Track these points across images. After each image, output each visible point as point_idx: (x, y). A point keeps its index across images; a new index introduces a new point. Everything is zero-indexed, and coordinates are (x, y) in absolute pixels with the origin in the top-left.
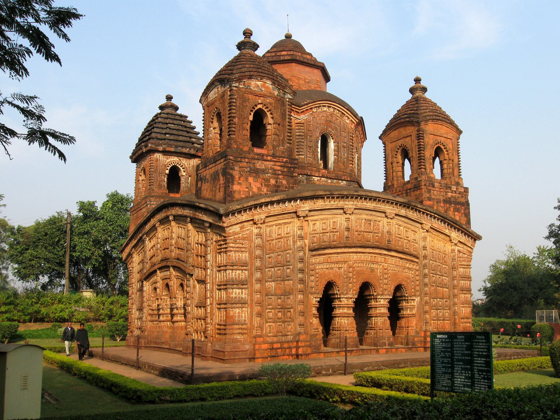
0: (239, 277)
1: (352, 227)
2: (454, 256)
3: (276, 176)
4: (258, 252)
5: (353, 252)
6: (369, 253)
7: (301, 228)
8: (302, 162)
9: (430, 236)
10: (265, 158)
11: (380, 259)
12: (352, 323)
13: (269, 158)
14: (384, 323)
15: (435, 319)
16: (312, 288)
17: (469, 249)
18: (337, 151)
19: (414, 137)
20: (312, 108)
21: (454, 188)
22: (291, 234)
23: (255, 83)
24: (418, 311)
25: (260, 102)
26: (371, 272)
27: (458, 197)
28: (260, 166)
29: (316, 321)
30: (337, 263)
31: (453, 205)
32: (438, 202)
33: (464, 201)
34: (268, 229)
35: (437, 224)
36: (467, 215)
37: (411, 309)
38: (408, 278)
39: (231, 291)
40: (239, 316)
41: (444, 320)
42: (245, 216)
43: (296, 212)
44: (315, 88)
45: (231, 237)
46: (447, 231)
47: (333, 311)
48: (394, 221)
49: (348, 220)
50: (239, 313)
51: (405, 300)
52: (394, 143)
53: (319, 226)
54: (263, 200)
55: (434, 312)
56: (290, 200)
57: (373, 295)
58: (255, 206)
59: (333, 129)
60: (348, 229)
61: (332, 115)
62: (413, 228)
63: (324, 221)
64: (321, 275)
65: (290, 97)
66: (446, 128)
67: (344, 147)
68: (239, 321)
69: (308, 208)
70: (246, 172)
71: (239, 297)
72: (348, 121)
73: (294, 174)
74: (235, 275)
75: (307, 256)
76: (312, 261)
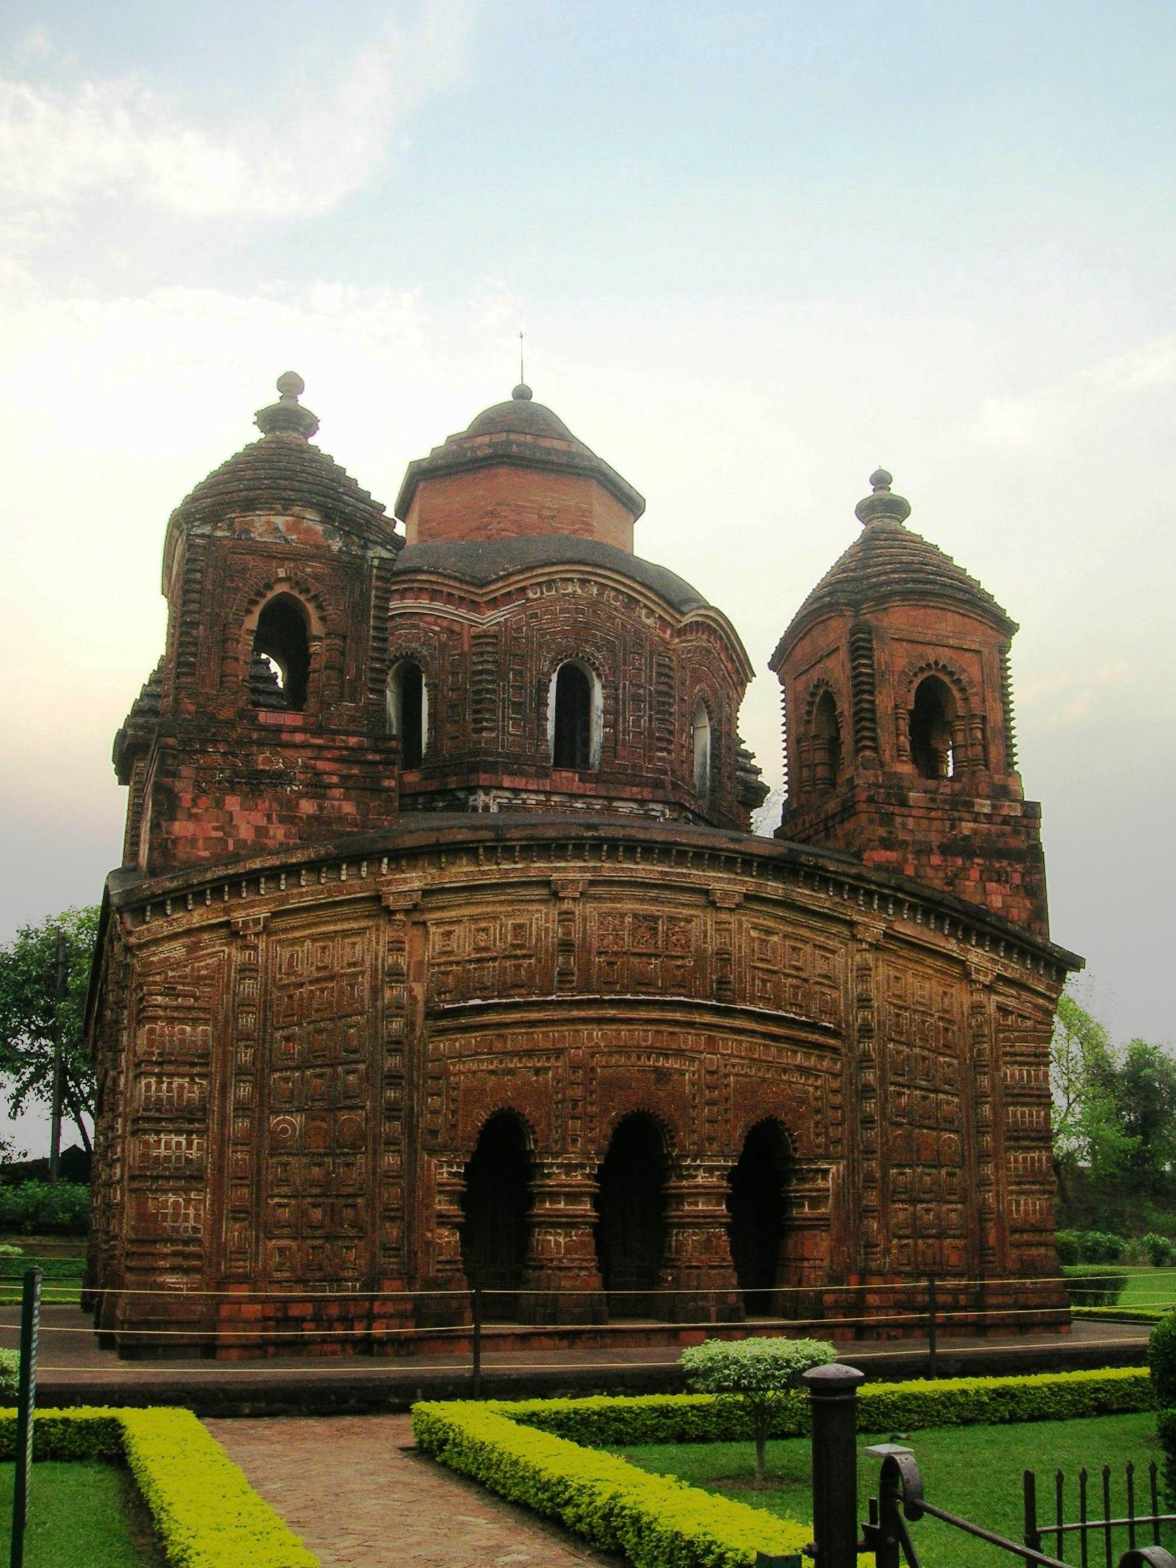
0: (180, 1096)
1: (584, 939)
2: (980, 1026)
3: (322, 791)
4: (248, 1021)
5: (585, 1021)
7: (397, 946)
8: (487, 753)
9: (889, 963)
10: (285, 737)
11: (689, 1040)
12: (583, 1245)
13: (299, 738)
14: (708, 1245)
16: (434, 1133)
17: (1041, 1001)
18: (612, 713)
19: (843, 655)
20: (524, 589)
21: (984, 806)
22: (368, 964)
23: (268, 522)
24: (837, 1206)
25: (282, 573)
26: (658, 1081)
28: (268, 761)
29: (448, 1237)
30: (529, 1053)
31: (977, 860)
32: (923, 850)
33: (1024, 846)
34: (284, 953)
36: (1035, 891)
37: (815, 1202)
38: (802, 1101)
39: (152, 1138)
40: (176, 1214)
42: (198, 917)
43: (377, 898)
44: (575, 531)
45: (158, 978)
46: (951, 946)
47: (531, 1205)
49: (566, 917)
50: (176, 1204)
51: (796, 1171)
52: (804, 678)
53: (463, 941)
54: (257, 864)
55: (901, 1212)
56: (354, 861)
57: (670, 1154)
58: (234, 883)
59: (598, 649)
60: (566, 946)
61: (594, 604)
62: (821, 939)
63: (483, 925)
64: (467, 1092)
65: (386, 555)
66: (957, 617)
67: (637, 699)
68: (175, 1230)
69: (417, 885)
70: (220, 782)
71: (178, 1158)
72: (649, 622)
73: (386, 783)
74: (169, 1090)
75: (418, 1033)
76: (436, 1049)
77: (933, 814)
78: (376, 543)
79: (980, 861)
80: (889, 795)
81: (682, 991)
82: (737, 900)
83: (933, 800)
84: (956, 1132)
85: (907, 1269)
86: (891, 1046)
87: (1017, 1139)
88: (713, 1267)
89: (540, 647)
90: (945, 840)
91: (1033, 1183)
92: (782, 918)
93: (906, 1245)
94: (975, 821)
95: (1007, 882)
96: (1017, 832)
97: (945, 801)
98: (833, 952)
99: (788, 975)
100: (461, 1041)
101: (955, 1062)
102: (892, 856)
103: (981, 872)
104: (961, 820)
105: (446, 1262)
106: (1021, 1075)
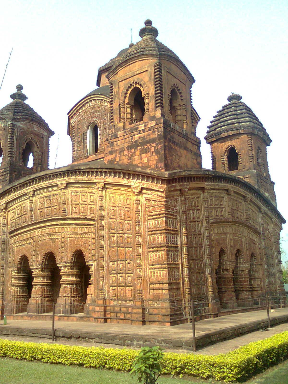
6: (49, 226)
11: (57, 229)
15: (115, 284)
17: (159, 193)
20: (78, 111)
27: (149, 135)
31: (138, 148)
35: (110, 179)
41: (126, 286)
48: (70, 189)
55: (113, 278)
59: (96, 118)
60: (31, 210)
69: (4, 202)
77: (125, 137)
78: (8, 121)
79: (140, 148)
80: (112, 136)
81: (56, 215)
82: (65, 185)
83: (125, 132)
84: (131, 247)
85: (115, 298)
86: (111, 220)
87: (152, 248)
88: (64, 297)
89: (83, 124)
90: (129, 145)
91: (158, 264)
92: (79, 187)
93: (114, 289)
94: (139, 134)
95: (149, 152)
96: (154, 132)
97: (129, 131)
98: (94, 193)
99: (81, 204)
100: (15, 238)
101: (131, 222)
102: (112, 156)
103: (140, 151)
104: (134, 135)
105: (13, 296)
106: (158, 223)
